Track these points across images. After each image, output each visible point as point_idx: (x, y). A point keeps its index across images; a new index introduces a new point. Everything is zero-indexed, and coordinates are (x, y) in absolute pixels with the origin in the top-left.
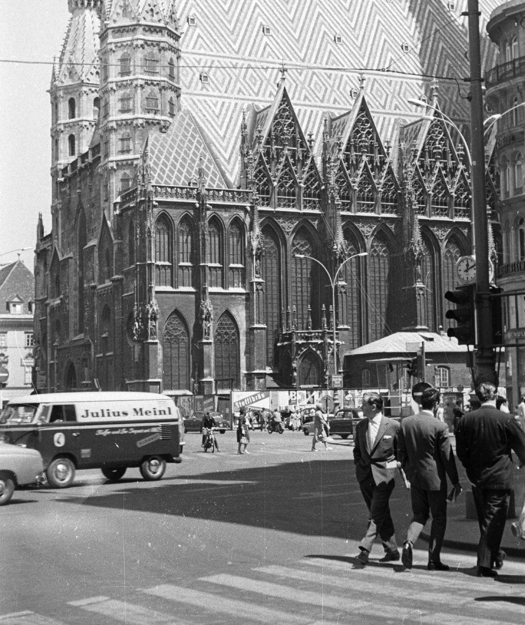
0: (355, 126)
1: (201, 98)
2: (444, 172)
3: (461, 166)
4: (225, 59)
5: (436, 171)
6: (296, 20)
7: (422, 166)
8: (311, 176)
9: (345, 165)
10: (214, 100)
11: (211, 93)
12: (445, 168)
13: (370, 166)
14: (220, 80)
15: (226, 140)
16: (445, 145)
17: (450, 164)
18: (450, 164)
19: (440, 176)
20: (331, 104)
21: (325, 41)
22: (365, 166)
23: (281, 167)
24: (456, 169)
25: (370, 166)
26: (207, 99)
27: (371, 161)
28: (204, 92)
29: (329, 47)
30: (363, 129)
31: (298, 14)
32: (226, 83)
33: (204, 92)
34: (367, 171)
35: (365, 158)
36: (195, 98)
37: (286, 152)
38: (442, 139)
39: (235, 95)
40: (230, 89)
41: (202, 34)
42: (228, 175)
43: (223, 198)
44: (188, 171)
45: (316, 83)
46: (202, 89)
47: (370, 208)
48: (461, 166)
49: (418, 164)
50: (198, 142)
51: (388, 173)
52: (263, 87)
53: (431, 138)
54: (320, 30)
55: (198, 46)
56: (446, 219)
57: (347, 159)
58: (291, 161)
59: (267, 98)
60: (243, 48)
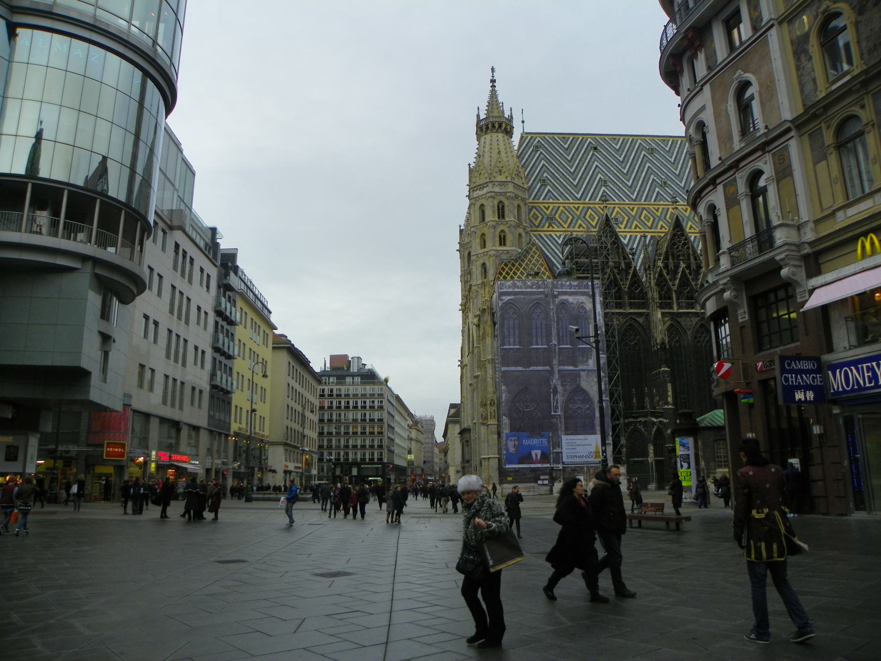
1: (547, 233)
8: (635, 282)
9: (664, 272)
11: (556, 229)
13: (687, 271)
14: (564, 219)
22: (683, 271)
25: (687, 271)
27: (688, 267)
28: (551, 228)
29: (657, 189)
32: (569, 220)
33: (551, 228)
34: (686, 275)
35: (683, 265)
45: (646, 215)
57: (666, 266)
58: (616, 271)
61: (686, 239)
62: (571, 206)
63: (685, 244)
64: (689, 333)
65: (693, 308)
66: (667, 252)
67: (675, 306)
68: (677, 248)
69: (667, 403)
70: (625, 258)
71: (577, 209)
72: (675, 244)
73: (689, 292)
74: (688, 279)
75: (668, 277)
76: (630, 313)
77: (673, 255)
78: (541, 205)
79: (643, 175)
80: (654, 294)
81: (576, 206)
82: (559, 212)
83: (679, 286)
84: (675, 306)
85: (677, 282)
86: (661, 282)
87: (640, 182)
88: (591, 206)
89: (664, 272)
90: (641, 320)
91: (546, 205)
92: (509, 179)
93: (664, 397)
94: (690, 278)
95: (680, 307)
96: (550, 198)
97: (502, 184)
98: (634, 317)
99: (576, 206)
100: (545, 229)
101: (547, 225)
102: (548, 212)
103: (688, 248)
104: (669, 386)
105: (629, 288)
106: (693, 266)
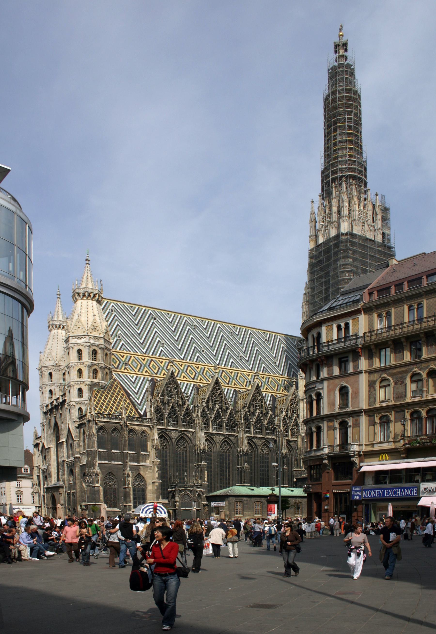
0: (212, 391)
1: (124, 374)
2: (261, 415)
3: (270, 413)
4: (138, 356)
5: (257, 414)
6: (179, 341)
7: (249, 411)
8: (187, 413)
9: (206, 409)
10: (132, 375)
11: (130, 371)
12: (262, 413)
14: (135, 365)
15: (139, 394)
16: (262, 402)
17: (264, 411)
18: (264, 411)
19: (258, 416)
20: (198, 381)
21: (195, 351)
23: (170, 408)
24: (267, 413)
26: (128, 375)
27: (221, 408)
28: (126, 371)
29: (198, 354)
30: (217, 393)
31: (180, 338)
35: (217, 406)
36: (120, 374)
37: (173, 401)
38: (260, 399)
39: (144, 373)
40: (141, 370)
41: (124, 343)
42: (139, 411)
43: (137, 421)
44: (116, 408)
46: (124, 370)
47: (220, 430)
48: (270, 413)
49: (247, 410)
50: (122, 394)
51: (230, 414)
52: (160, 370)
53: (254, 399)
54: (192, 346)
55: (122, 349)
56: (262, 436)
57: (207, 406)
59: (162, 376)
60: (148, 352)
61: (221, 392)
62: (140, 357)
63: (220, 394)
64: (218, 444)
65: (221, 431)
66: (208, 398)
67: (211, 429)
68: (215, 396)
69: (204, 481)
70: (182, 399)
71: (144, 360)
72: (214, 394)
73: (220, 422)
74: (220, 415)
75: (208, 412)
76: (183, 431)
77: (212, 400)
78: (118, 354)
79: (188, 343)
80: (199, 421)
81: (143, 358)
82: (131, 360)
83: (215, 418)
84: (211, 429)
85: (213, 416)
86: (204, 415)
87: (186, 347)
88: (154, 359)
89: (206, 409)
90: (189, 435)
91: (122, 354)
92: (102, 336)
93: (202, 478)
94: (221, 414)
95: (213, 430)
96: (124, 349)
97: (95, 338)
98: (185, 433)
99: (143, 358)
100: (122, 370)
101: (123, 368)
102: (123, 359)
103: (222, 397)
104: (206, 472)
105: (183, 416)
106: (224, 408)
